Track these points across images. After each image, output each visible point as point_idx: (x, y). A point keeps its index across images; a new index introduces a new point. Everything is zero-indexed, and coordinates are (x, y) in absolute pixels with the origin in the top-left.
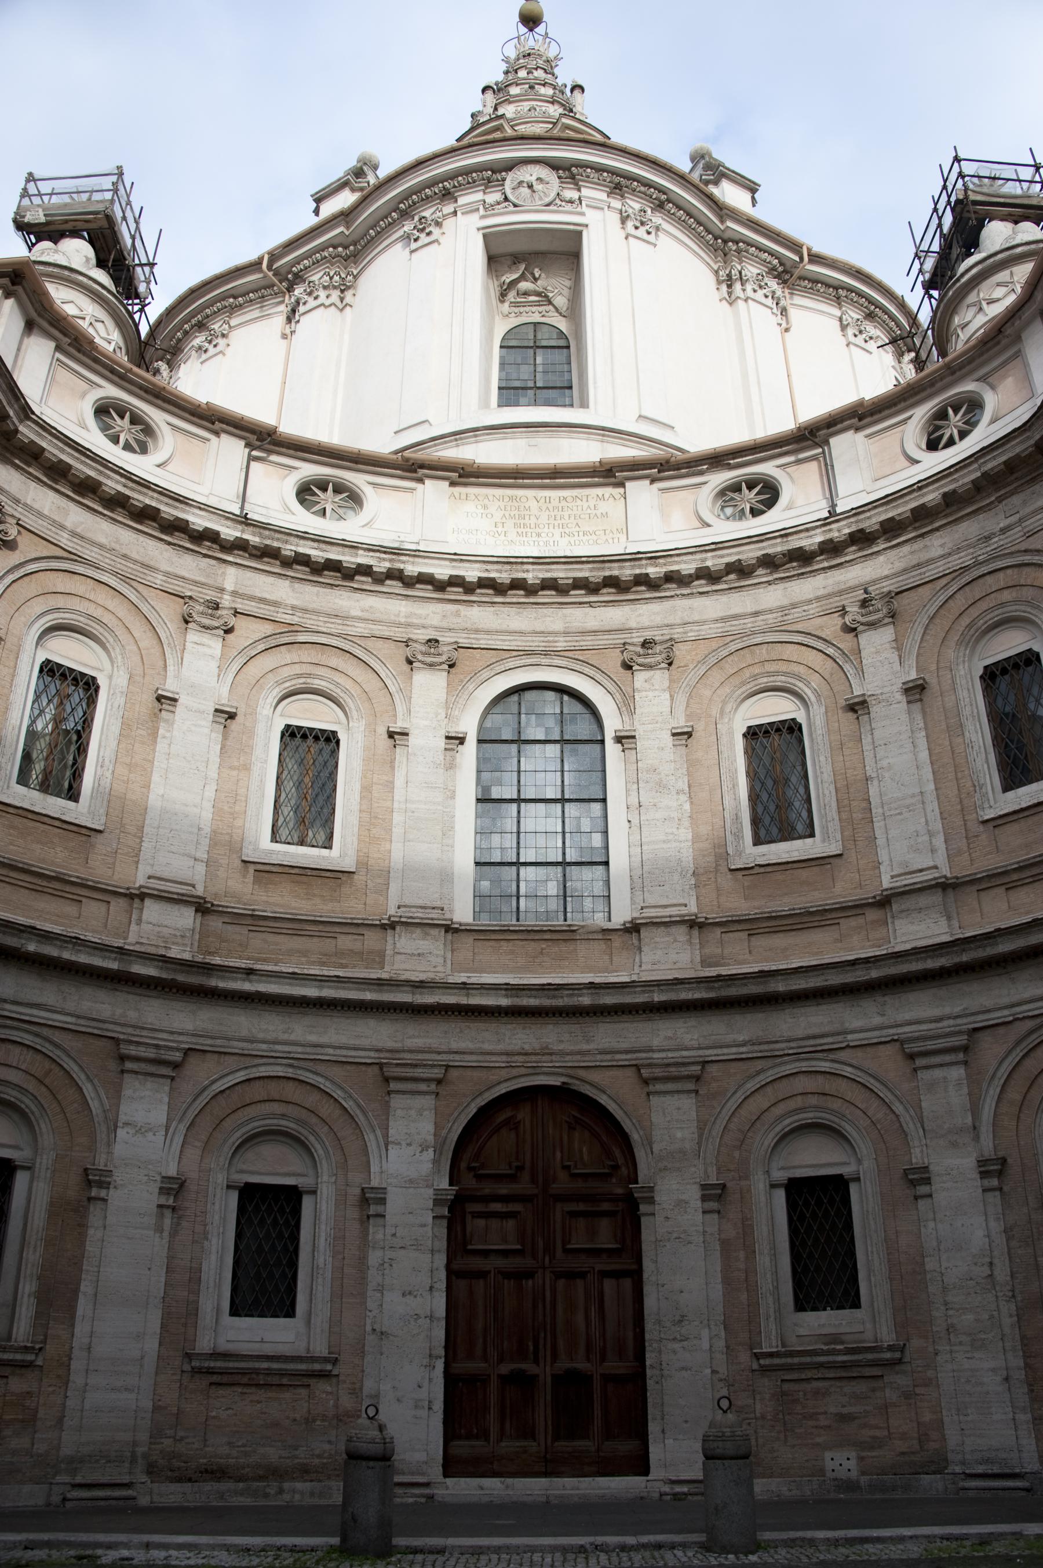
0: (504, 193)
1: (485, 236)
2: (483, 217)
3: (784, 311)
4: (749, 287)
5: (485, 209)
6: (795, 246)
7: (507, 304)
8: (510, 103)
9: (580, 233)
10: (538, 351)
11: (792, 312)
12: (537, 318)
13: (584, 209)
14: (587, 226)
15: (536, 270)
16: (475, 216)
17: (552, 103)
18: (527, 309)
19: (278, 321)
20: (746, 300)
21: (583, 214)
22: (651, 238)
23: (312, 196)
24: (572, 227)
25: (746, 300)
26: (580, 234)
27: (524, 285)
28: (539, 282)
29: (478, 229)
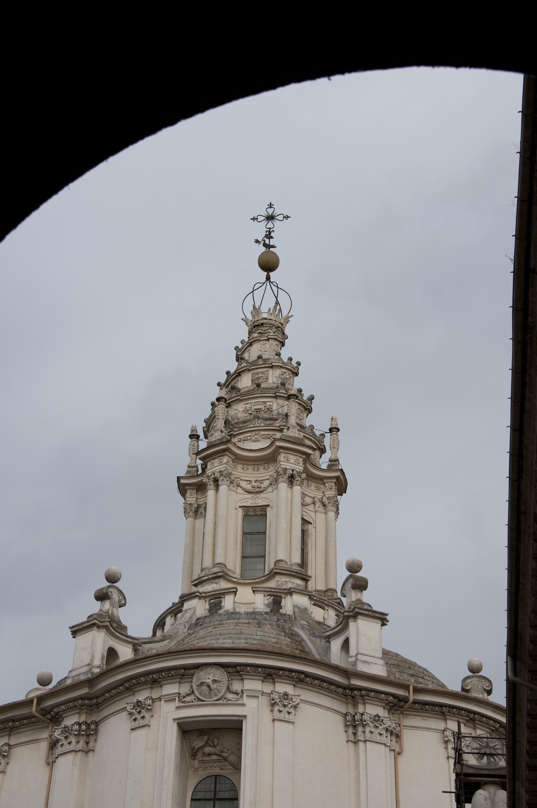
0: (192, 687)
1: (179, 724)
2: (178, 708)
3: (398, 736)
4: (368, 729)
5: (180, 701)
6: (406, 687)
7: (197, 762)
8: (241, 401)
9: (242, 721)
10: (217, 802)
11: (407, 735)
12: (216, 771)
13: (245, 700)
14: (246, 716)
15: (215, 740)
16: (172, 706)
17: (276, 397)
18: (210, 764)
19: (44, 746)
20: (365, 741)
21: (243, 705)
22: (291, 718)
23: (70, 628)
24: (236, 718)
25: (365, 741)
26: (241, 722)
27: (208, 750)
28: (217, 747)
29: (174, 720)
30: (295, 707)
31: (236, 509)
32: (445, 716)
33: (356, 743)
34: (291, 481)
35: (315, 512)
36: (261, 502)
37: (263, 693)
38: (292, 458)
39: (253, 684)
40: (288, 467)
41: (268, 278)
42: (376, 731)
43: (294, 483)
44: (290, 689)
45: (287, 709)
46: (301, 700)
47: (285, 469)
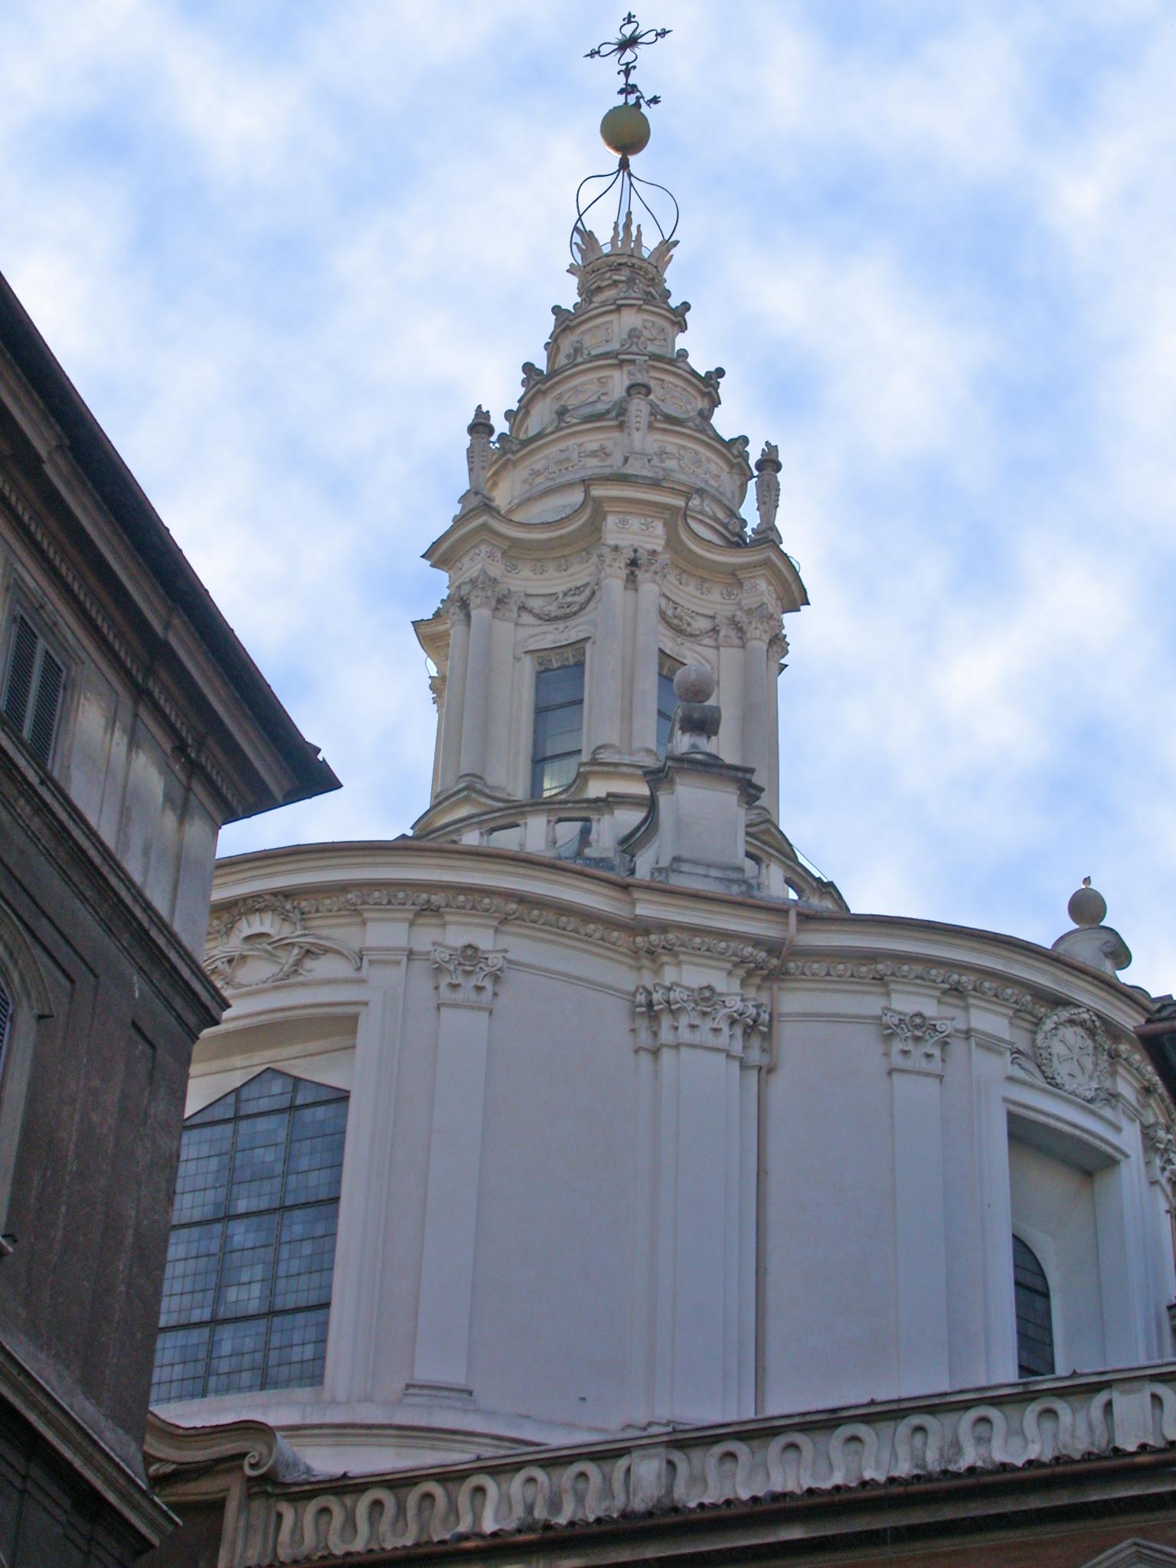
4: (684, 1021)
11: (788, 1033)
14: (366, 1004)
20: (677, 1047)
25: (677, 1047)
30: (496, 978)
31: (517, 659)
32: (886, 985)
33: (655, 1053)
34: (632, 573)
35: (718, 648)
36: (573, 636)
37: (411, 954)
38: (635, 523)
39: (386, 932)
40: (621, 543)
41: (624, 165)
42: (707, 1025)
43: (640, 577)
44: (484, 939)
45: (474, 981)
46: (510, 962)
47: (616, 548)
